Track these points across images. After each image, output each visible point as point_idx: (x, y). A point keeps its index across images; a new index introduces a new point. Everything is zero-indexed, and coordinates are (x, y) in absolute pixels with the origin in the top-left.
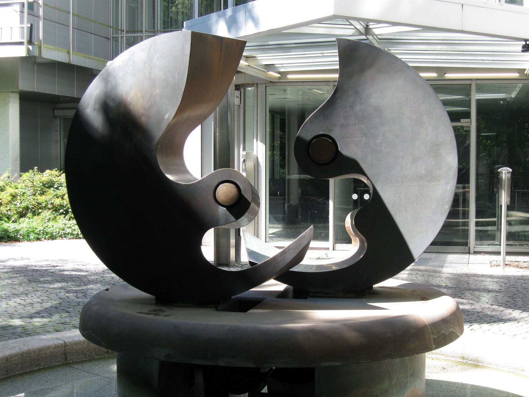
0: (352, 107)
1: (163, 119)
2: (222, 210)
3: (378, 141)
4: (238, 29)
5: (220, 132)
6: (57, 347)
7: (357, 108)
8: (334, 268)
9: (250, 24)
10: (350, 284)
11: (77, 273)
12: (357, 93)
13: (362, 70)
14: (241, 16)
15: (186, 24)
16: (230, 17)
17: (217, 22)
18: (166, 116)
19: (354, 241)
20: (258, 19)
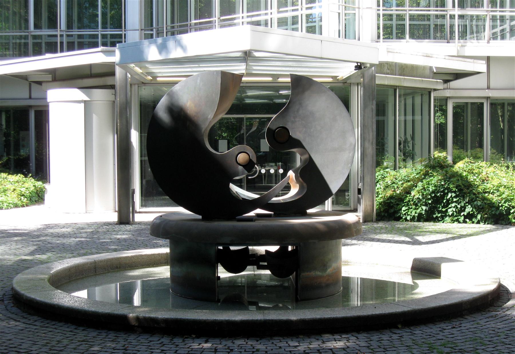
0: (298, 111)
1: (207, 118)
2: (240, 168)
3: (312, 130)
4: (168, 52)
5: (120, 123)
6: (91, 263)
7: (301, 112)
8: (282, 202)
9: (179, 50)
10: (297, 208)
11: (131, 211)
12: (300, 104)
13: (303, 91)
14: (171, 44)
15: (119, 46)
16: (161, 44)
17: (149, 47)
18: (209, 117)
19: (293, 187)
20: (186, 47)
